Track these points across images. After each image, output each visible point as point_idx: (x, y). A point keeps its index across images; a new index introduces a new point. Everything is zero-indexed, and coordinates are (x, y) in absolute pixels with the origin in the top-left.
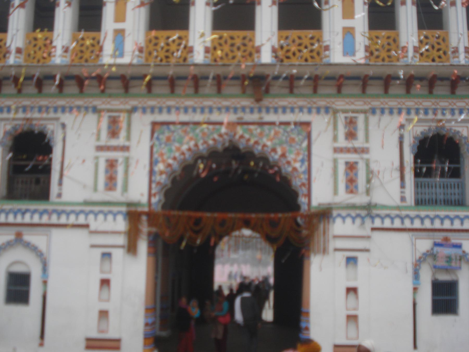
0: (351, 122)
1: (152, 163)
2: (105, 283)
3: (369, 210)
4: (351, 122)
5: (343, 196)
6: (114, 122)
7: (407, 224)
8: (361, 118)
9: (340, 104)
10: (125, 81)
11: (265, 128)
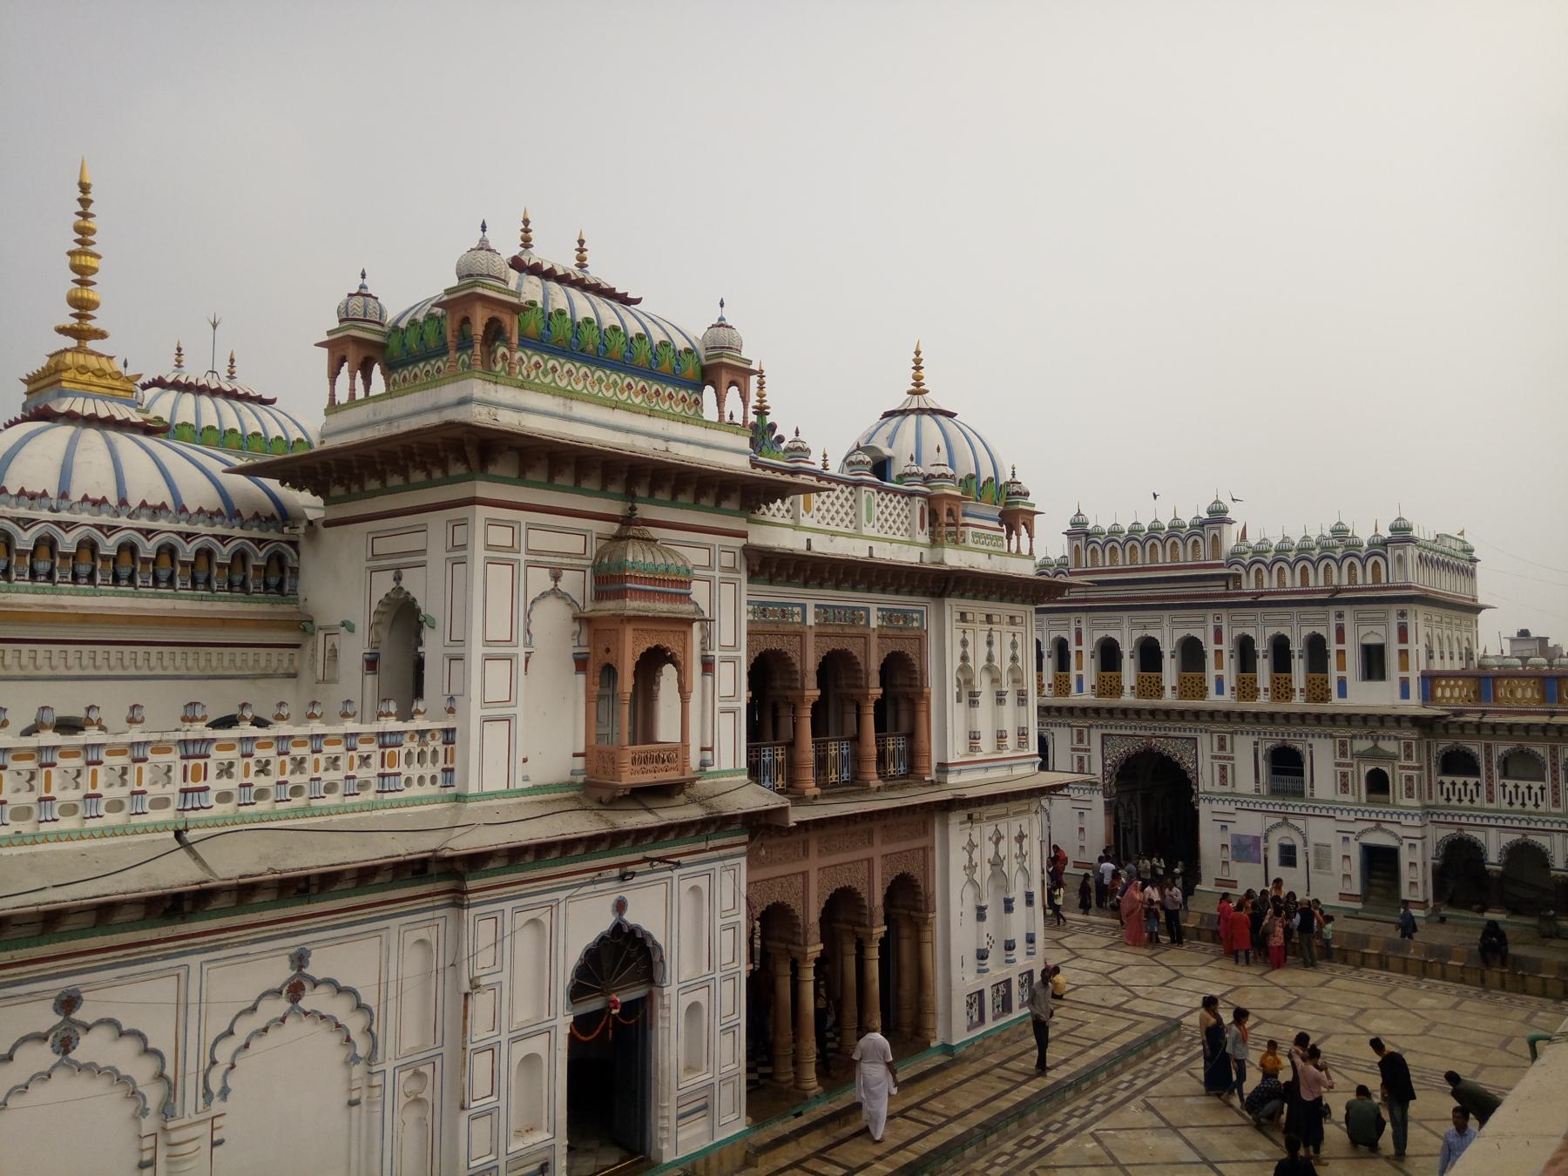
0: (1222, 739)
2: (1082, 830)
3: (1233, 796)
4: (1222, 739)
5: (1218, 788)
6: (1080, 733)
8: (1228, 737)
9: (1214, 727)
10: (1085, 711)
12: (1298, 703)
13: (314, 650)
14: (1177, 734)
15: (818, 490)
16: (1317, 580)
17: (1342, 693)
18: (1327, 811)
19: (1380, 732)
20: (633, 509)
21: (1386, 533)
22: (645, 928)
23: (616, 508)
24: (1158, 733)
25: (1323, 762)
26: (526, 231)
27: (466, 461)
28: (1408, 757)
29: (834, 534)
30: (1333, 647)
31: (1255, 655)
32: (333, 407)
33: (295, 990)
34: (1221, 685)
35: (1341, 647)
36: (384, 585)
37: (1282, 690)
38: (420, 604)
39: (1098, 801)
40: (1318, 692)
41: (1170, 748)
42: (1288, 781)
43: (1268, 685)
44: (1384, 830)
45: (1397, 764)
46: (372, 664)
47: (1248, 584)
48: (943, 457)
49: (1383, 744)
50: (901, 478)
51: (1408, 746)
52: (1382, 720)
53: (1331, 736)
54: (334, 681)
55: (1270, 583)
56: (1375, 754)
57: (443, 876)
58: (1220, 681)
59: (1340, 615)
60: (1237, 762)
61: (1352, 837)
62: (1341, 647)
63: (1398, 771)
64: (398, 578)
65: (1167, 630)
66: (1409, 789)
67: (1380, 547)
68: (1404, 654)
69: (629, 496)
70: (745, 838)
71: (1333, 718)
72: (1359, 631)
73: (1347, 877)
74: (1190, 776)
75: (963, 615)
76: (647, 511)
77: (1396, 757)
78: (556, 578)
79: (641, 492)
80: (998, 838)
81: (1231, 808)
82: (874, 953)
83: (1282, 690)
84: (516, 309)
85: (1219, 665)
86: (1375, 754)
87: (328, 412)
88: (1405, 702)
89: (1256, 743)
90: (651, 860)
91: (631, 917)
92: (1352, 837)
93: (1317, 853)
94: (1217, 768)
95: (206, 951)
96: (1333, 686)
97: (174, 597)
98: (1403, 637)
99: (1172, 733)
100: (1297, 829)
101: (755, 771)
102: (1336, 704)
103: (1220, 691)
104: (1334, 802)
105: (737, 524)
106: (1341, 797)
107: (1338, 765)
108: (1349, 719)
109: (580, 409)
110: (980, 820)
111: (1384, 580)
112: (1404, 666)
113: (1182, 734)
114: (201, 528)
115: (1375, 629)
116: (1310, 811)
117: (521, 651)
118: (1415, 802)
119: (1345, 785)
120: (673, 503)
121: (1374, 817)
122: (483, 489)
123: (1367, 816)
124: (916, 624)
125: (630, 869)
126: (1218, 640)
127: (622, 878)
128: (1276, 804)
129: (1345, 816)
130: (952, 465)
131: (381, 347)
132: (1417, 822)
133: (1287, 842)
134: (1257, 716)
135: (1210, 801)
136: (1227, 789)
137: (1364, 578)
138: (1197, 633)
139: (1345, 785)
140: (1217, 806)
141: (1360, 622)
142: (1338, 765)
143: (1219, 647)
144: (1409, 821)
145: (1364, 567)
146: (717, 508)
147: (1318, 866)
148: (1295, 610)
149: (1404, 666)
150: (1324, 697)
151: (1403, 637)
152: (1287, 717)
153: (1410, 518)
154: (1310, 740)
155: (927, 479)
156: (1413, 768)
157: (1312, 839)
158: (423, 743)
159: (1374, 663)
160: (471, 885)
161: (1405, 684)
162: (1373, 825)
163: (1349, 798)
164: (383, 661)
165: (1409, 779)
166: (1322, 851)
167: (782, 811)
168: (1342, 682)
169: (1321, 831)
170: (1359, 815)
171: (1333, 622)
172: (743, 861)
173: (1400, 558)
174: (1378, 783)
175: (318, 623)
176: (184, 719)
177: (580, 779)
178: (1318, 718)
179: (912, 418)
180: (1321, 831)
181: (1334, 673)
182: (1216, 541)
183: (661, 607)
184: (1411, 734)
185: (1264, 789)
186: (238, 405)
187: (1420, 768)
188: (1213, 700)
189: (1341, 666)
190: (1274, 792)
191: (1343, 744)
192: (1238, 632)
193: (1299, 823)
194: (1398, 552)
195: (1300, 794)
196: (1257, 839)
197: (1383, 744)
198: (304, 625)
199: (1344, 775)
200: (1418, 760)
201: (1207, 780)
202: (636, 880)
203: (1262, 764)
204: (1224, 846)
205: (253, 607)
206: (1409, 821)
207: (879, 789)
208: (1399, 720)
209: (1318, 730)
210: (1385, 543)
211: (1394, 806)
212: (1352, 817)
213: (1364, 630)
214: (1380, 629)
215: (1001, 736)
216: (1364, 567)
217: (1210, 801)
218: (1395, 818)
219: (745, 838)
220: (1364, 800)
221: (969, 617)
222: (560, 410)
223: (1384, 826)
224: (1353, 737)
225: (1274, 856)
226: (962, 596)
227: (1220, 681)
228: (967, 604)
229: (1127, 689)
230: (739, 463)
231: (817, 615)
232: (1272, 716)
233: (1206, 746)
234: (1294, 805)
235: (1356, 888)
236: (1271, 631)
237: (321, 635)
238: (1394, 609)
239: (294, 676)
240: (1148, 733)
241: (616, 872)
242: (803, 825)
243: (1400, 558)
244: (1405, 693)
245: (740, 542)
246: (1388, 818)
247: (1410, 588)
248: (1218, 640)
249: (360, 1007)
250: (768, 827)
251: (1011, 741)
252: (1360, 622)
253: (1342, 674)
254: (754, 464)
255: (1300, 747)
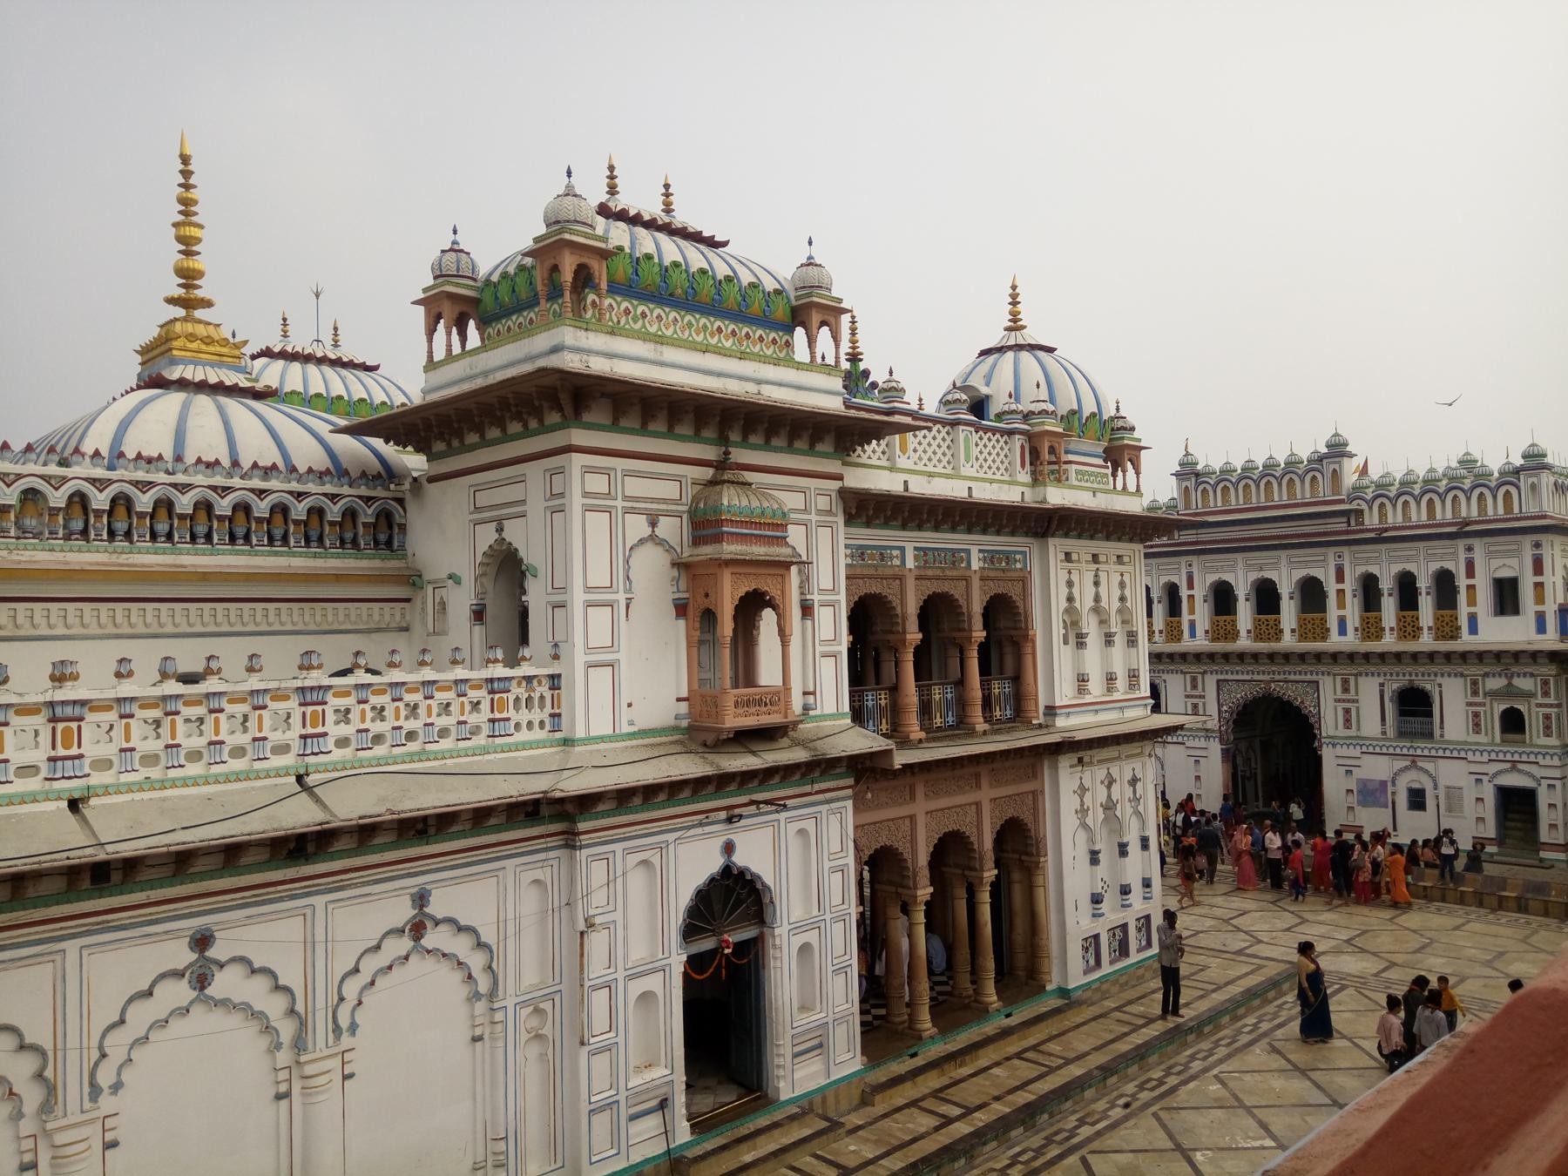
1: (1220, 705)
2: (1198, 778)
3: (1359, 740)
5: (1342, 732)
6: (1194, 680)
7: (1384, 750)
9: (1336, 669)
10: (1198, 657)
11: (1287, 684)
12: (1426, 642)
13: (424, 603)
14: (1298, 677)
15: (914, 429)
16: (1444, 513)
17: (1473, 629)
18: (1458, 752)
19: (1514, 669)
20: (727, 453)
21: (1518, 461)
22: (754, 869)
23: (710, 453)
24: (1277, 677)
25: (1453, 701)
26: (612, 177)
27: (561, 409)
28: (1546, 694)
29: (931, 475)
30: (1462, 582)
31: (1379, 594)
32: (431, 365)
33: (417, 929)
34: (1343, 624)
35: (1471, 582)
36: (487, 536)
37: (1409, 629)
38: (522, 553)
39: (1215, 748)
40: (1448, 629)
41: (1291, 693)
42: (1416, 723)
43: (1393, 624)
44: (1520, 771)
45: (1534, 701)
46: (479, 615)
47: (1372, 520)
48: (1044, 394)
49: (1517, 682)
50: (999, 417)
51: (1545, 683)
52: (1517, 656)
53: (1462, 675)
54: (444, 633)
55: (1395, 517)
56: (1509, 692)
57: (555, 818)
58: (1342, 622)
59: (1470, 549)
60: (1362, 704)
61: (1485, 779)
62: (1471, 582)
63: (1534, 709)
64: (500, 530)
65: (1284, 571)
66: (1547, 728)
67: (1512, 475)
68: (1539, 586)
69: (723, 440)
70: (851, 781)
71: (1464, 656)
72: (1490, 564)
73: (1480, 820)
74: (1312, 720)
75: (1068, 555)
76: (740, 455)
77: (1531, 695)
78: (653, 524)
79: (735, 436)
80: (1110, 782)
81: (1356, 752)
82: (985, 897)
83: (1409, 629)
84: (605, 255)
85: (1341, 605)
86: (1509, 692)
87: (427, 369)
88: (1541, 637)
89: (1382, 685)
90: (757, 803)
91: (739, 859)
92: (1485, 779)
93: (1448, 797)
94: (1340, 713)
95: (330, 891)
96: (1464, 622)
97: (288, 554)
98: (1538, 568)
99: (1292, 677)
100: (1426, 772)
101: (858, 715)
102: (1466, 641)
103: (1343, 631)
104: (1466, 743)
105: (832, 466)
106: (1474, 738)
107: (1469, 704)
108: (1481, 656)
109: (670, 354)
110: (1091, 763)
111: (1516, 510)
112: (1540, 599)
113: (1303, 677)
114: (311, 487)
115: (1508, 561)
116: (1440, 753)
117: (621, 597)
118: (1553, 741)
119: (1477, 725)
120: (767, 446)
121: (1509, 757)
122: (578, 437)
123: (1501, 757)
124: (1018, 566)
125: (737, 811)
126: (1340, 577)
127: (729, 820)
128: (1404, 746)
129: (1478, 757)
130: (1052, 400)
131: (475, 302)
132: (1556, 762)
133: (1416, 786)
134: (1383, 657)
135: (1334, 745)
136: (1352, 732)
137: (1495, 509)
138: (1318, 573)
139: (1477, 725)
140: (1340, 751)
141: (1490, 555)
142: (1469, 704)
143: (1340, 586)
144: (1548, 761)
145: (1495, 497)
146: (811, 451)
147: (1450, 809)
148: (1421, 545)
149: (1540, 599)
150: (1454, 634)
151: (1538, 568)
152: (1415, 656)
153: (1544, 444)
154: (1439, 680)
155: (1027, 416)
156: (1551, 706)
157: (1442, 782)
158: (530, 689)
159: (1506, 597)
160: (582, 826)
161: (1541, 619)
162: (1508, 765)
163: (1482, 738)
164: (490, 613)
165: (1547, 717)
166: (1453, 794)
167: (887, 753)
168: (1473, 619)
169: (1451, 773)
170: (1493, 756)
171: (1462, 556)
172: (849, 804)
173: (1533, 487)
174: (1513, 723)
175: (426, 577)
176: (301, 668)
177: (685, 723)
178: (1448, 657)
179: (1010, 355)
180: (1451, 773)
181: (1463, 610)
182: (1336, 476)
183: (758, 551)
184: (1550, 670)
185: (1391, 733)
186: (344, 372)
187: (1559, 706)
188: (1335, 642)
189: (1472, 601)
190: (1402, 734)
191: (1475, 683)
192: (1361, 570)
193: (1429, 766)
194: (1530, 480)
195: (1429, 735)
196: (1384, 784)
197: (1517, 682)
198: (413, 580)
199: (1476, 715)
200: (1557, 697)
201: (1330, 723)
202: (743, 822)
203: (1389, 706)
204: (1349, 791)
205: (364, 563)
206: (1548, 761)
207: (985, 733)
208: (1534, 656)
209: (1447, 669)
210: (1517, 472)
211: (1532, 745)
212: (1485, 757)
213: (1495, 563)
214: (1514, 562)
215: (1111, 678)
216: (1495, 497)
217: (1334, 745)
218: (1532, 758)
219: (851, 781)
220: (1498, 739)
221: (1074, 556)
222: (651, 356)
223: (1520, 766)
224: (1486, 675)
225: (1402, 800)
226: (1066, 535)
227: (1342, 622)
228: (1071, 544)
229: (1243, 633)
230: (833, 404)
231: (916, 558)
232: (1398, 656)
233: (1329, 688)
234: (1422, 748)
235: (1490, 831)
236: (1396, 568)
237: (430, 589)
238: (1527, 541)
239: (406, 629)
240: (1266, 677)
241: (723, 815)
242: (908, 768)
243: (1533, 487)
244: (1541, 627)
245: (836, 485)
246: (1524, 758)
247: (1544, 517)
248: (1340, 577)
249: (480, 945)
250: (873, 770)
251: (1121, 683)
252: (1490, 555)
253: (1472, 610)
254: (847, 407)
255: (1428, 687)
